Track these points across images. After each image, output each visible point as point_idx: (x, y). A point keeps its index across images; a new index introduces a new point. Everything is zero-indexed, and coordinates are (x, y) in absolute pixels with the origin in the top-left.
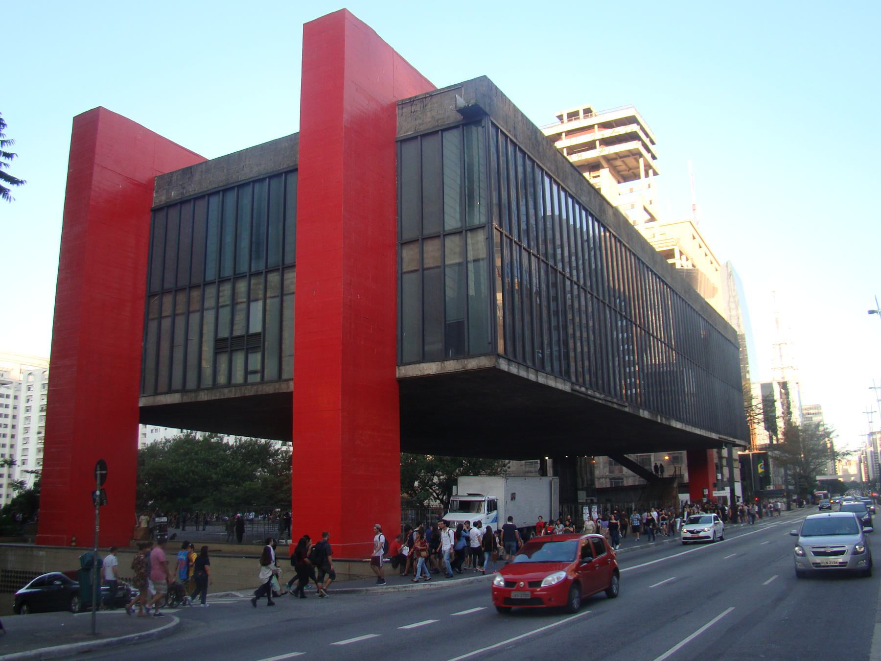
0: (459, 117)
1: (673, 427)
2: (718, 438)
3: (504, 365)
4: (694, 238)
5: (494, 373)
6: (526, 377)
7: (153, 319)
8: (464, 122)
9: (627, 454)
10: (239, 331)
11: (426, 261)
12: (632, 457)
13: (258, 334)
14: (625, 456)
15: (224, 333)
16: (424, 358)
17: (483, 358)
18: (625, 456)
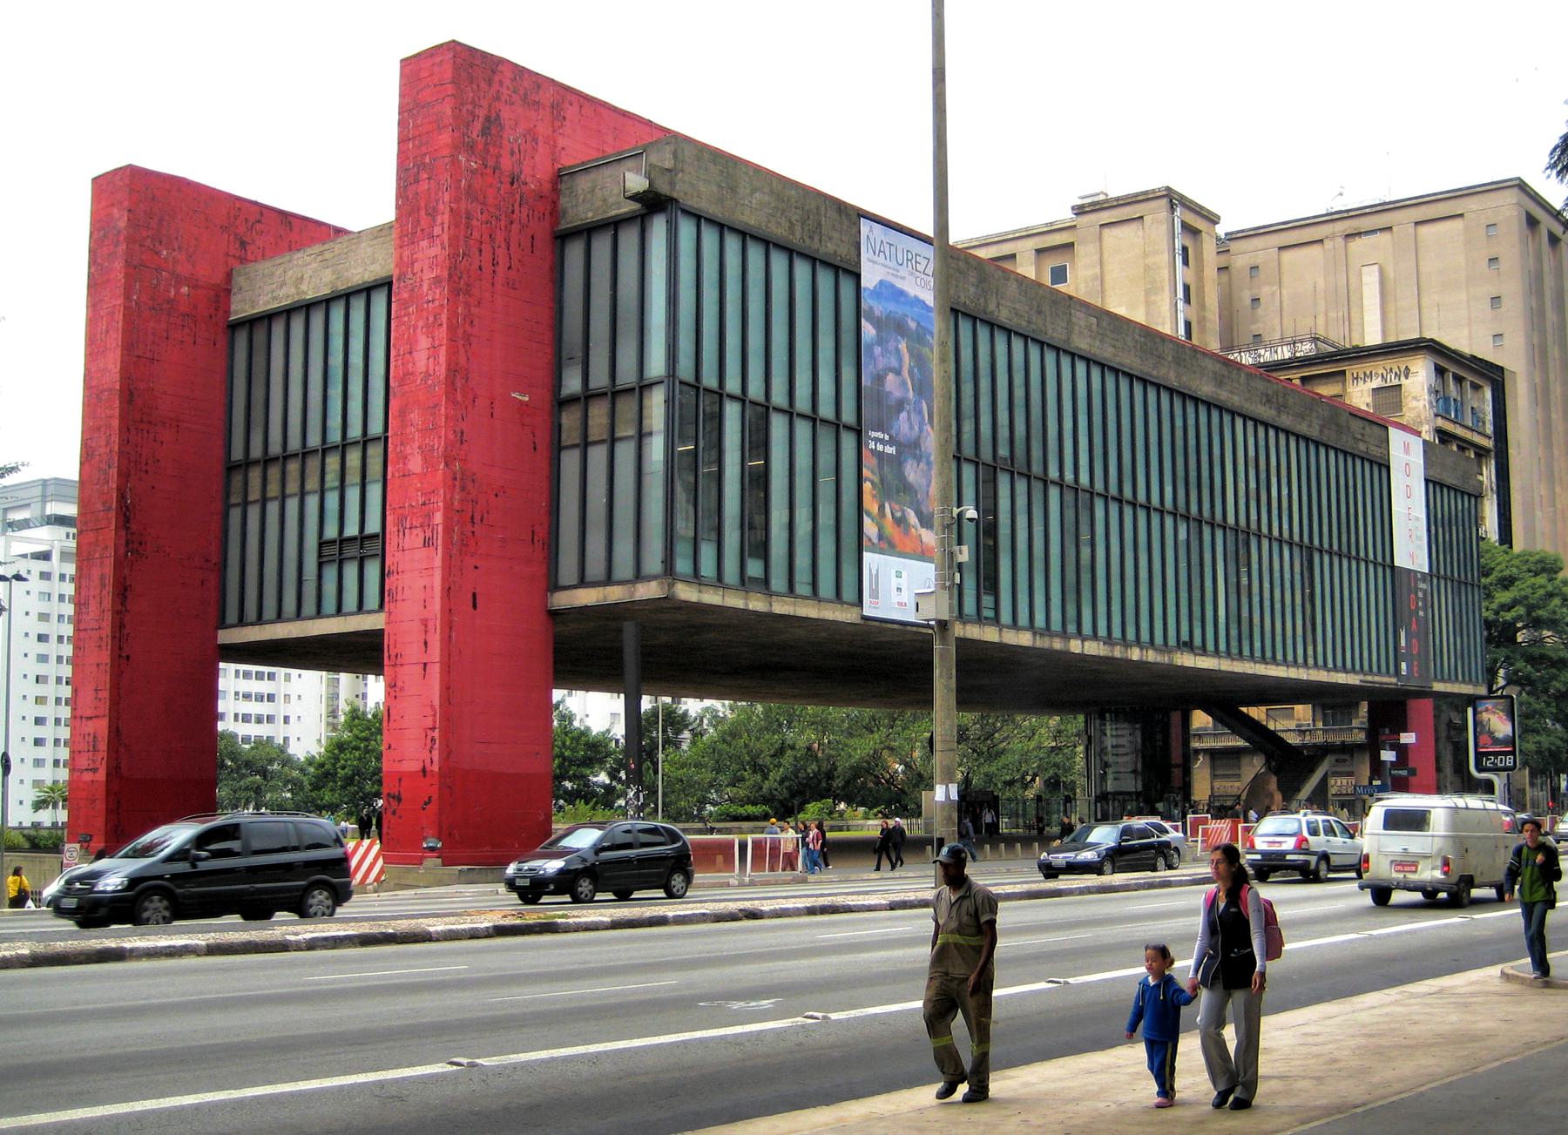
0: (634, 206)
1: (1183, 668)
2: (1357, 683)
3: (686, 593)
4: (1532, 222)
5: (667, 604)
6: (741, 607)
7: (235, 505)
8: (644, 211)
9: (1248, 704)
10: (352, 530)
11: (590, 431)
12: (1256, 713)
13: (375, 536)
14: (1244, 709)
15: (331, 532)
16: (583, 582)
17: (654, 584)
18: (1244, 709)
